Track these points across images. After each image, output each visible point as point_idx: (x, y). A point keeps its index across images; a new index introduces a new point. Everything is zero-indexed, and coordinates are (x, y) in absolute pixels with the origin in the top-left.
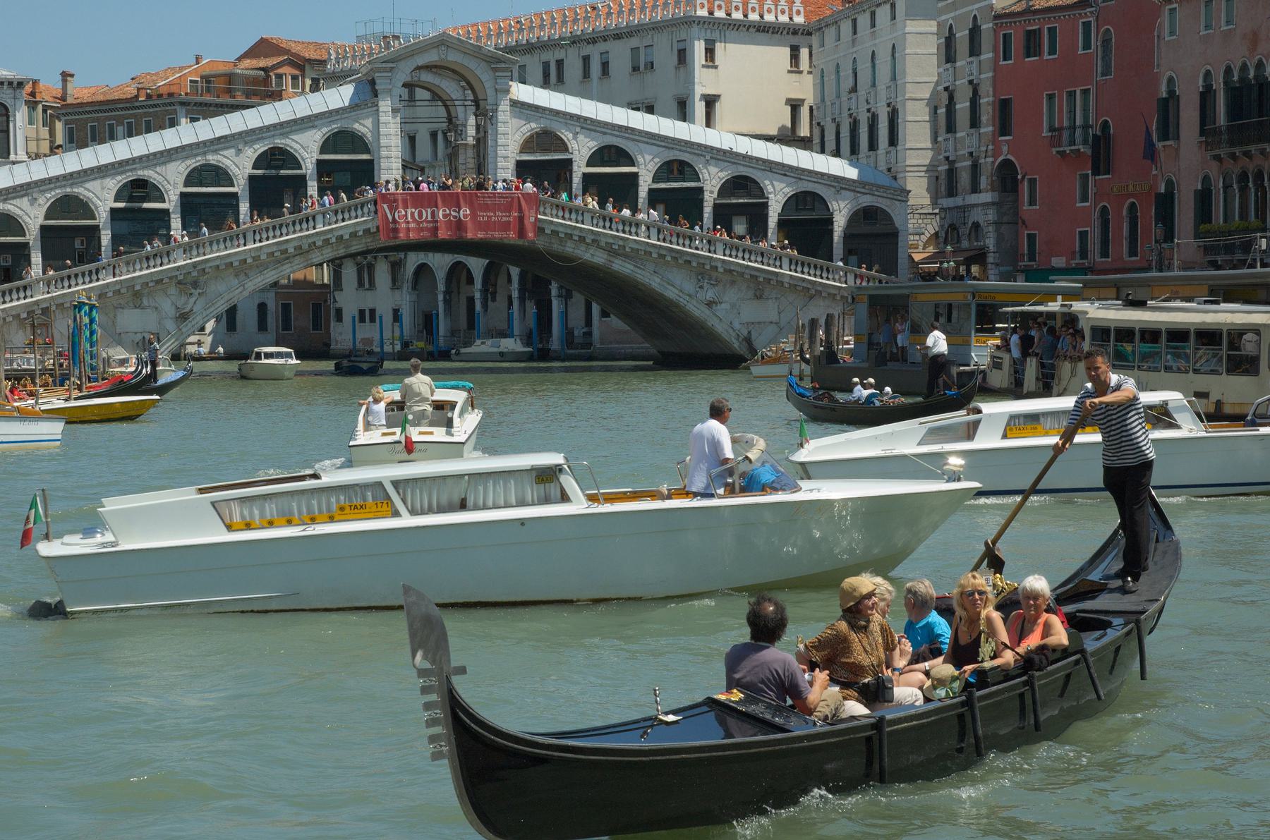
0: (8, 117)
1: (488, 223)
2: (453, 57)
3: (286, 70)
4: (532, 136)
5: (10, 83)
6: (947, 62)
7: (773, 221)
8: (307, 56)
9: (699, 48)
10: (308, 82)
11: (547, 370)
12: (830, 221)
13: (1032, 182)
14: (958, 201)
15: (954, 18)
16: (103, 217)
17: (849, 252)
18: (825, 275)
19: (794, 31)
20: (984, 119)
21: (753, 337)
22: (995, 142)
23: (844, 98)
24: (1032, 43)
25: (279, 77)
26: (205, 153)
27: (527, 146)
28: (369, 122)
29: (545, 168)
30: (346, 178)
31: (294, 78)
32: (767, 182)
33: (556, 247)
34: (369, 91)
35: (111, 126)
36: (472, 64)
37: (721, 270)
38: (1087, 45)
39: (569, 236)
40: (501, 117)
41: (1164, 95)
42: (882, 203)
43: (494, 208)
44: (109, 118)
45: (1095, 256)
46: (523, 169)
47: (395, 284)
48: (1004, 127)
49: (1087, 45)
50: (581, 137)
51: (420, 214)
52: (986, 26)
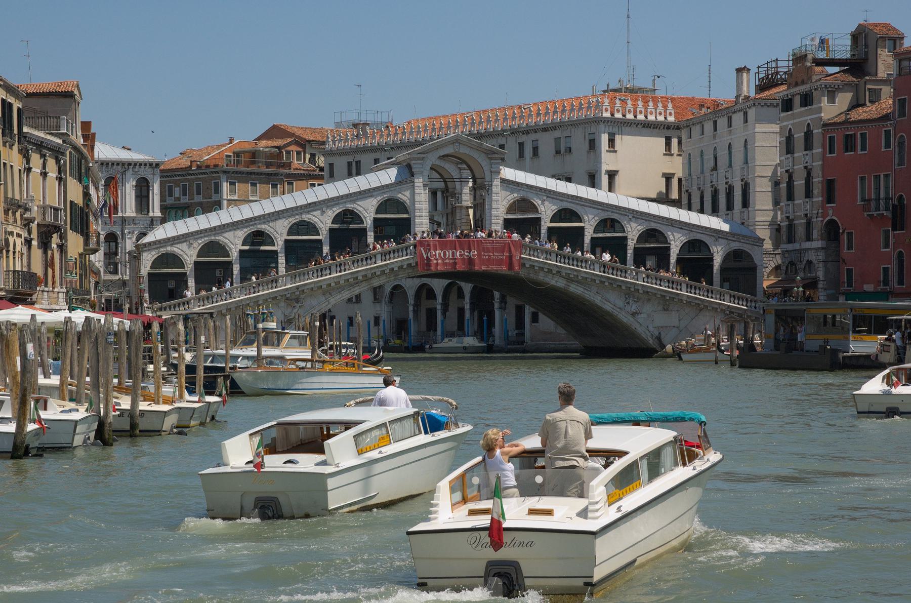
0: (148, 187)
1: (488, 260)
2: (463, 150)
3: (293, 148)
4: (514, 202)
5: (151, 165)
7: (673, 259)
8: (306, 137)
9: (605, 138)
10: (308, 156)
11: (495, 358)
12: (712, 259)
13: (850, 235)
14: (796, 246)
15: (793, 124)
16: (234, 255)
17: (723, 280)
18: (710, 295)
19: (667, 126)
20: (815, 192)
21: (662, 336)
22: (823, 207)
23: (707, 173)
24: (849, 143)
25: (288, 152)
26: (301, 214)
27: (510, 210)
28: (408, 193)
29: (523, 223)
30: (391, 230)
31: (298, 153)
32: (669, 233)
33: (532, 276)
34: (408, 172)
35: (170, 188)
37: (641, 291)
38: (888, 145)
39: (542, 269)
40: (494, 189)
42: (746, 248)
43: (494, 250)
44: (170, 182)
45: (894, 283)
46: (509, 224)
49: (888, 145)
50: (546, 203)
51: (445, 254)
52: (817, 131)
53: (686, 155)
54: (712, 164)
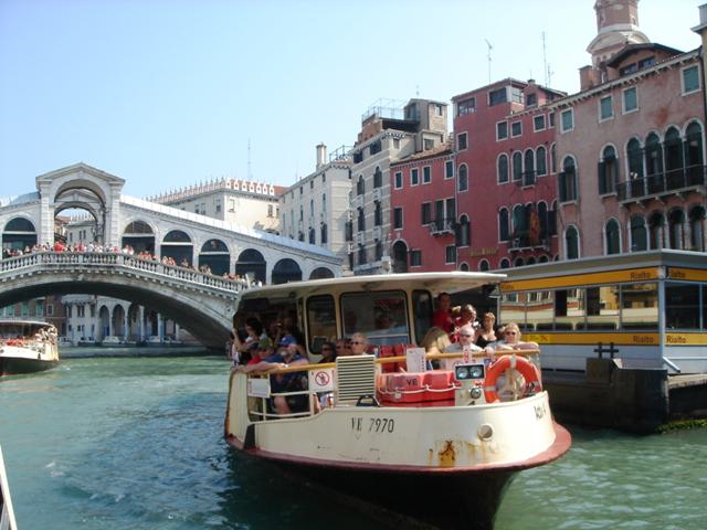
2: (87, 177)
6: (359, 194)
20: (385, 220)
27: (129, 229)
36: (98, 182)
38: (449, 174)
40: (114, 212)
41: (562, 171)
46: (126, 242)
47: (93, 314)
48: (397, 222)
49: (449, 174)
52: (385, 171)
53: (281, 216)
54: (299, 217)
